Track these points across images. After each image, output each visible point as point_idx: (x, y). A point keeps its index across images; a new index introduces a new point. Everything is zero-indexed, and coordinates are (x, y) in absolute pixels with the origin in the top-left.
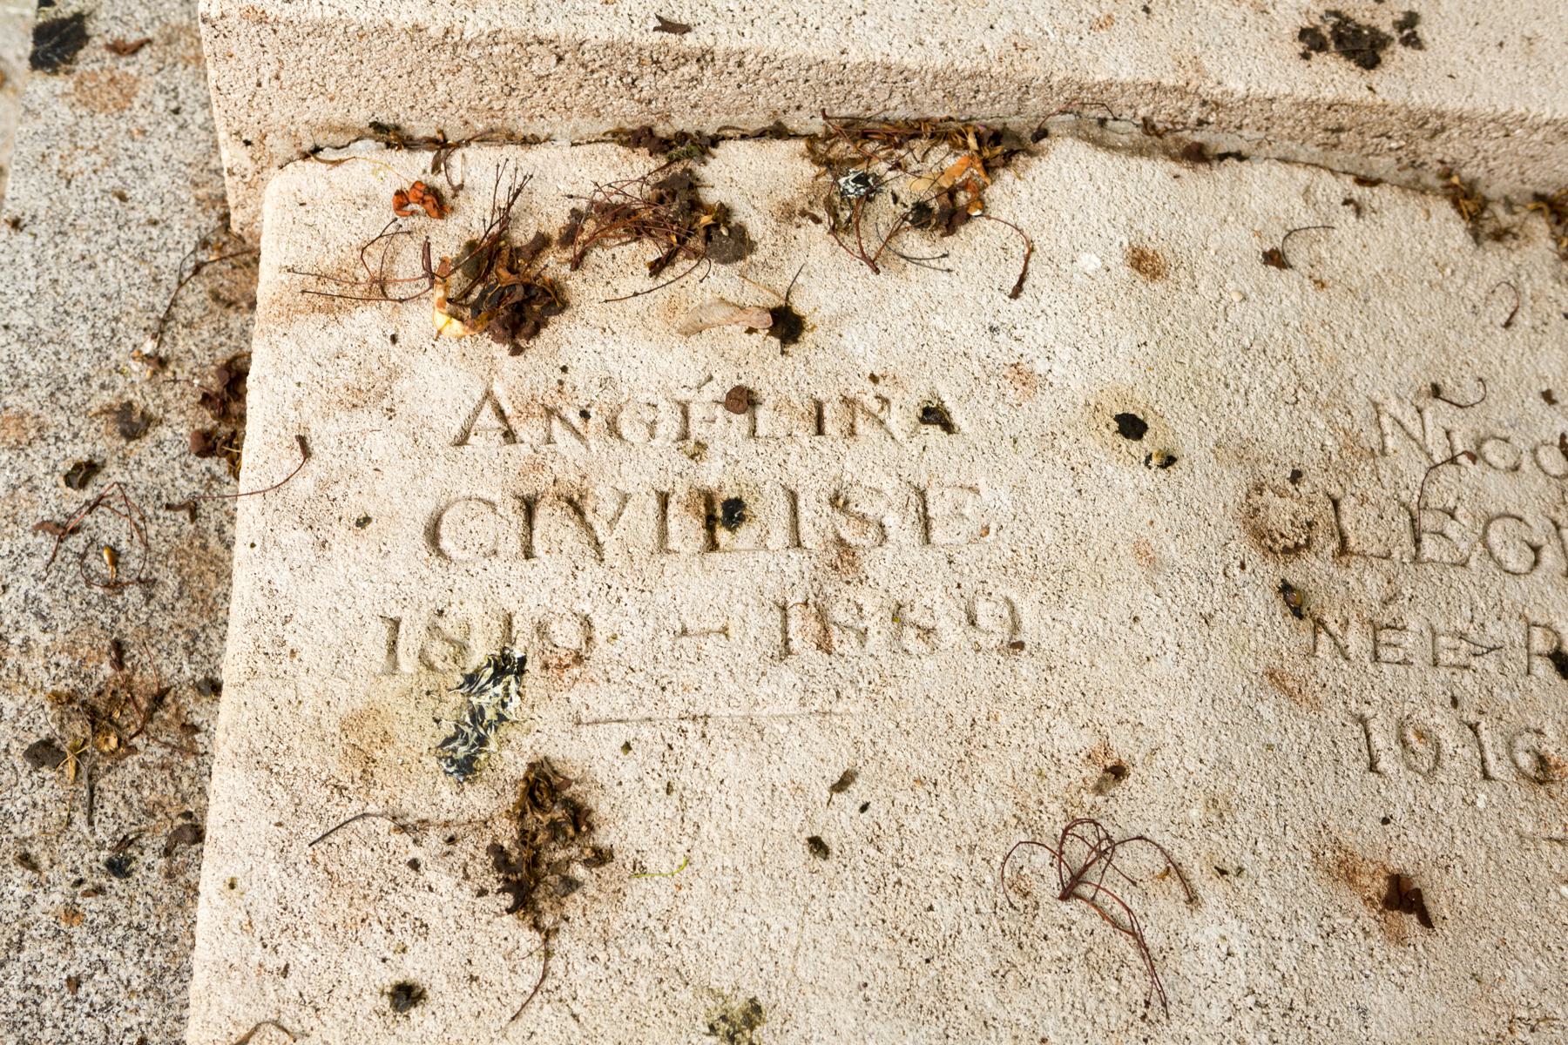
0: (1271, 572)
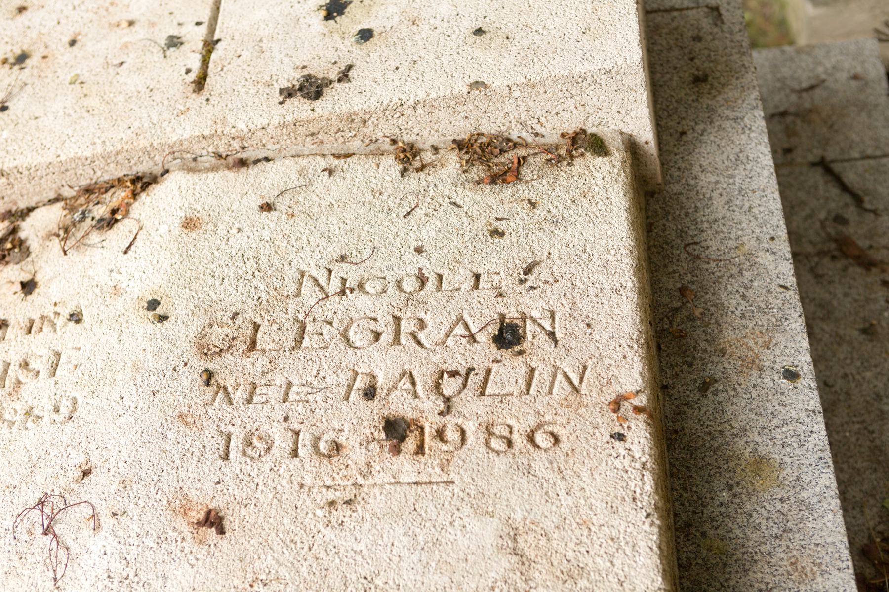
0: (200, 364)
